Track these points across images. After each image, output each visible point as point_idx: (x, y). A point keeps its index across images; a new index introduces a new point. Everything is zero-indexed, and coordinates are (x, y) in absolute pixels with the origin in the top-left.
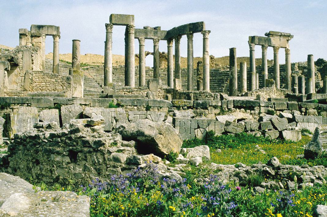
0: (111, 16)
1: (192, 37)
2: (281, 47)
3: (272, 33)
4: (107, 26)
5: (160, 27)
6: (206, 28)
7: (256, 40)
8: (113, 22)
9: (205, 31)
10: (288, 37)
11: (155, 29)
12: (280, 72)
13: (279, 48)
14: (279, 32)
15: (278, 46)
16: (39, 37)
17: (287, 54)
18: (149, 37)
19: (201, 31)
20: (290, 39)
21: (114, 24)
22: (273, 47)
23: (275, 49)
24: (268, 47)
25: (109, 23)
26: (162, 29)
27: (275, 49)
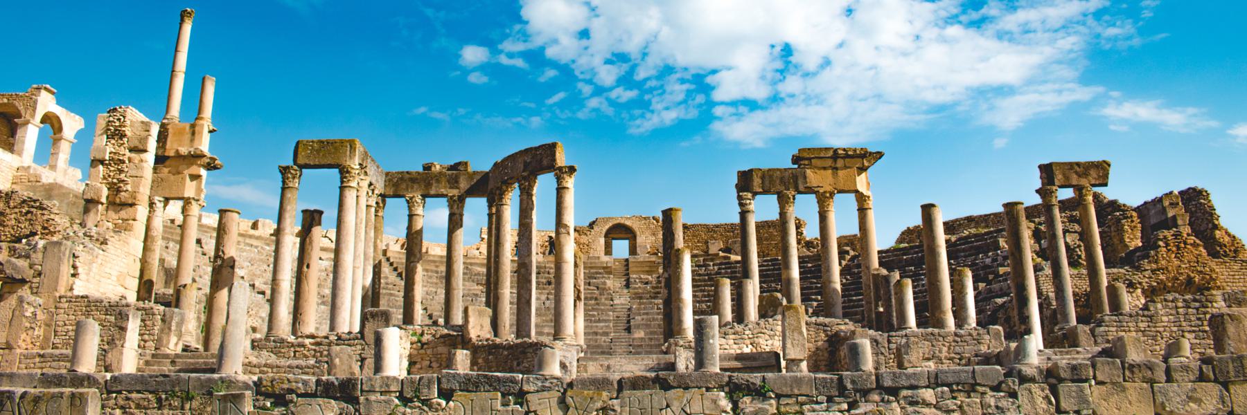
0: (298, 143)
1: (531, 187)
2: (840, 192)
3: (805, 155)
4: (284, 170)
5: (466, 163)
6: (562, 159)
7: (757, 182)
8: (301, 161)
9: (560, 169)
10: (862, 159)
11: (452, 168)
12: (949, 259)
13: (832, 194)
14: (827, 149)
15: (829, 188)
16: (132, 205)
17: (862, 211)
18: (432, 192)
19: (550, 166)
20: (866, 164)
21: (302, 167)
22: (816, 193)
23: (823, 201)
24: (798, 196)
25: (290, 163)
26: (470, 169)
27: (823, 201)
